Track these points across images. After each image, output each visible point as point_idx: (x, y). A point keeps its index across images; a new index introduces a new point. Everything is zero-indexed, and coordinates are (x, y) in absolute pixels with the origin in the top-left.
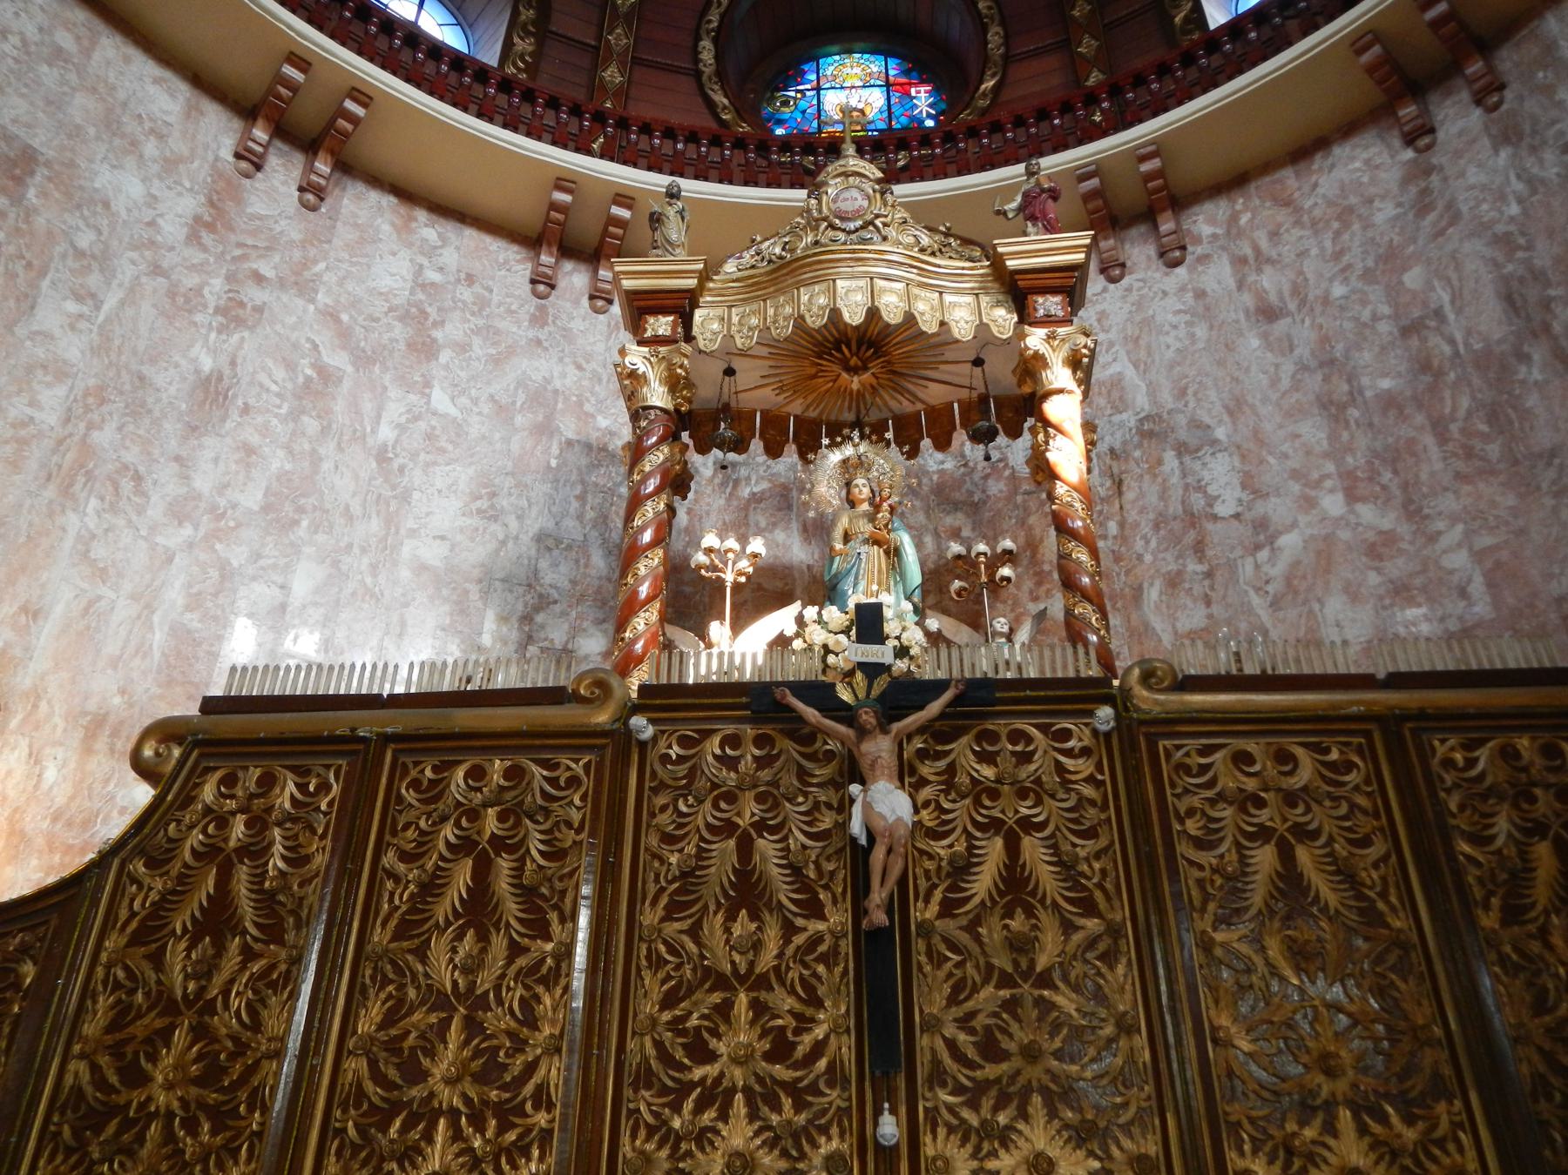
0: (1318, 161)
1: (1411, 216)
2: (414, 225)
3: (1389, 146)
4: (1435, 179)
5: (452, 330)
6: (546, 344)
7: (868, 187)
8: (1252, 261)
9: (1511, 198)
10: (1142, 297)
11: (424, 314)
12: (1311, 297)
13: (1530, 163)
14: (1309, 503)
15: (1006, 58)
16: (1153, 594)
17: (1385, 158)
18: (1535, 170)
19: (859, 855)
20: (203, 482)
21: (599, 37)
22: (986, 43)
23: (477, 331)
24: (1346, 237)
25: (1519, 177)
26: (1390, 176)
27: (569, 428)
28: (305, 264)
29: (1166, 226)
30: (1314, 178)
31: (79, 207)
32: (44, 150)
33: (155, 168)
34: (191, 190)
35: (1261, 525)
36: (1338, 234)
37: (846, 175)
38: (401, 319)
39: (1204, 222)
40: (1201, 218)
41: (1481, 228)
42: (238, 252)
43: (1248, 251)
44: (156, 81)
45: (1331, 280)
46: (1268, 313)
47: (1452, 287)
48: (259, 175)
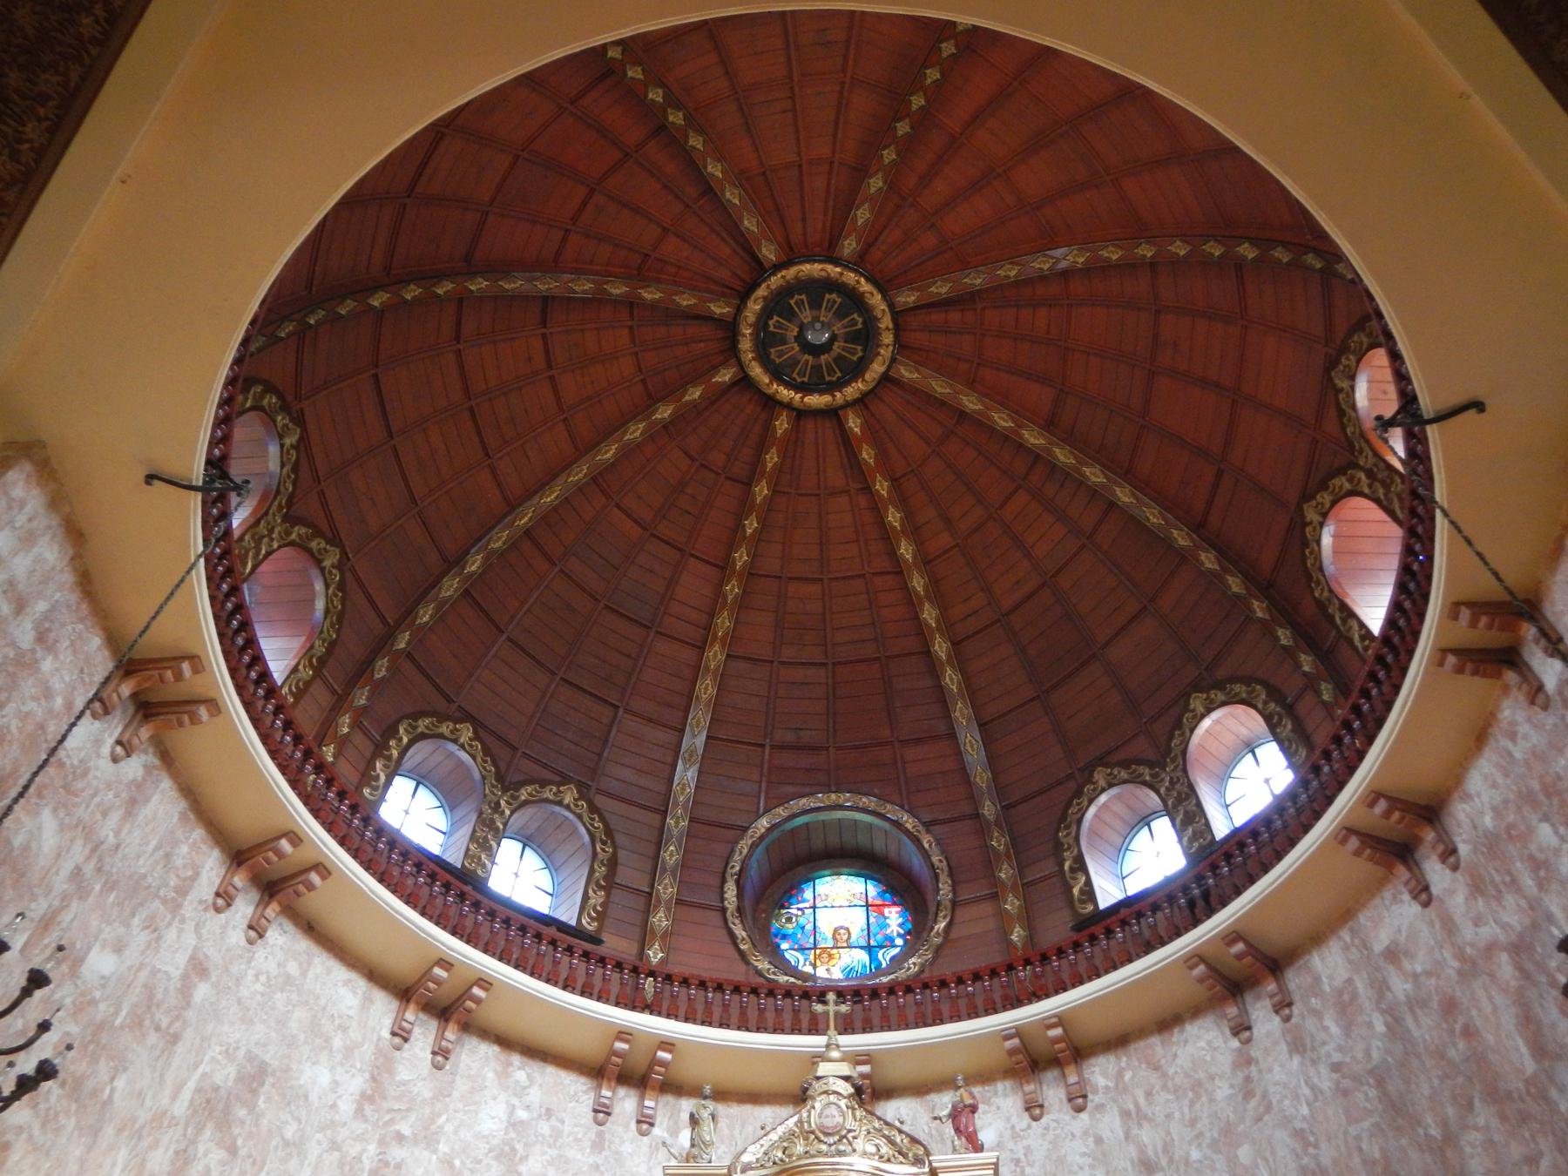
1: (1240, 1097)
2: (511, 1069)
3: (1223, 1033)
4: (1253, 1068)
6: (602, 1168)
7: (843, 1103)
8: (1134, 1115)
9: (1303, 1099)
10: (1057, 1136)
11: (513, 1149)
12: (1177, 1157)
13: (1312, 1072)
15: (955, 904)
17: (1219, 1042)
18: (1316, 1080)
21: (652, 886)
22: (938, 890)
23: (551, 1163)
24: (1198, 1106)
25: (1306, 1083)
26: (1225, 1060)
28: (432, 1120)
29: (1073, 1079)
30: (1174, 1049)
31: (289, 1104)
32: (272, 1062)
33: (339, 1057)
34: (360, 1070)
36: (1192, 1105)
37: (826, 1092)
38: (497, 1158)
39: (1100, 1072)
40: (1097, 1069)
41: (1285, 1121)
42: (387, 1118)
43: (1131, 1107)
44: (346, 983)
45: (1190, 1144)
47: (1270, 1169)
48: (406, 1046)
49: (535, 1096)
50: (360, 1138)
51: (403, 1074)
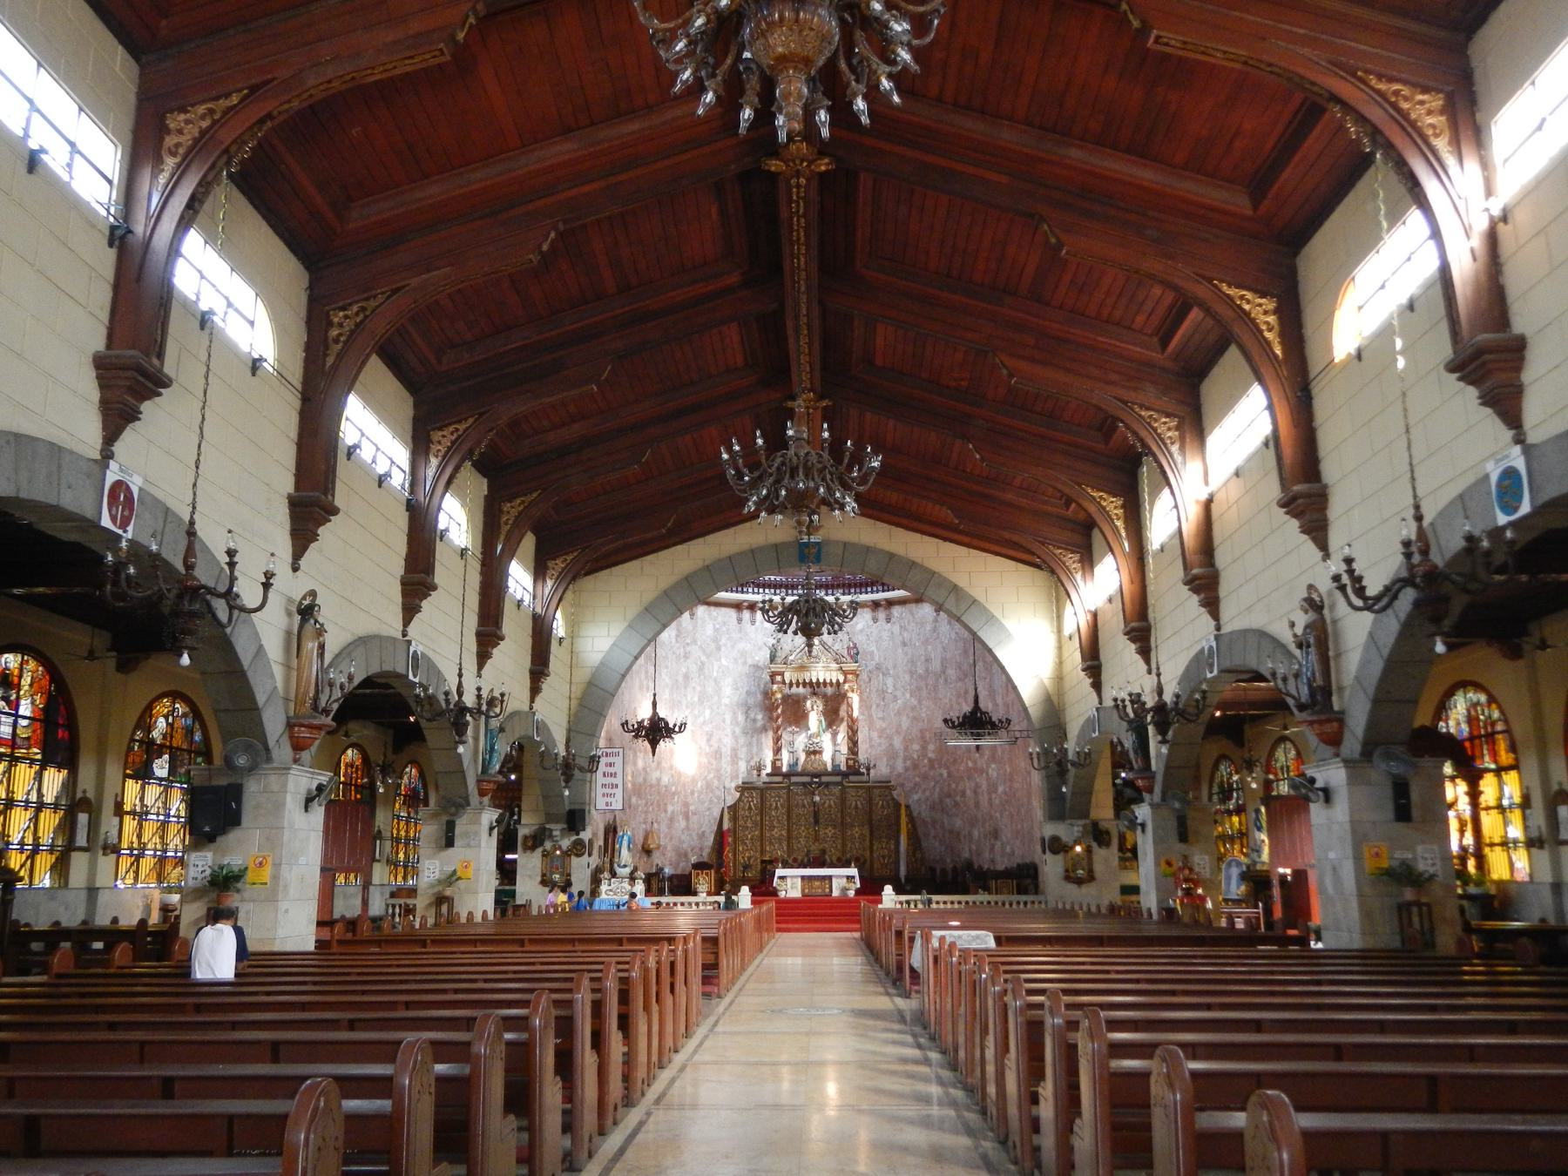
0: (920, 605)
5: (723, 641)
14: (904, 694)
16: (874, 707)
19: (815, 803)
20: (689, 699)
26: (931, 619)
27: (750, 662)
35: (895, 696)
41: (941, 643)
46: (904, 644)
49: (720, 619)
50: (679, 648)
51: (684, 625)
